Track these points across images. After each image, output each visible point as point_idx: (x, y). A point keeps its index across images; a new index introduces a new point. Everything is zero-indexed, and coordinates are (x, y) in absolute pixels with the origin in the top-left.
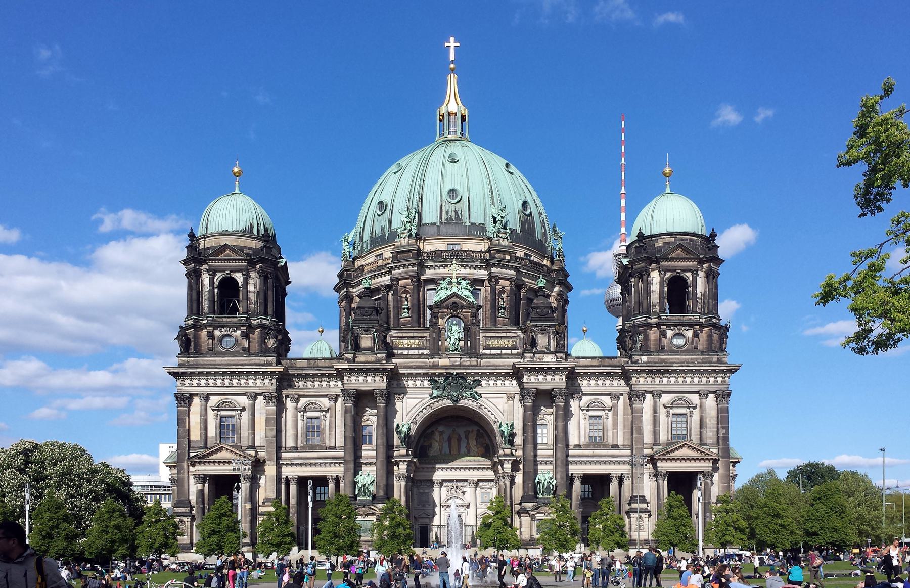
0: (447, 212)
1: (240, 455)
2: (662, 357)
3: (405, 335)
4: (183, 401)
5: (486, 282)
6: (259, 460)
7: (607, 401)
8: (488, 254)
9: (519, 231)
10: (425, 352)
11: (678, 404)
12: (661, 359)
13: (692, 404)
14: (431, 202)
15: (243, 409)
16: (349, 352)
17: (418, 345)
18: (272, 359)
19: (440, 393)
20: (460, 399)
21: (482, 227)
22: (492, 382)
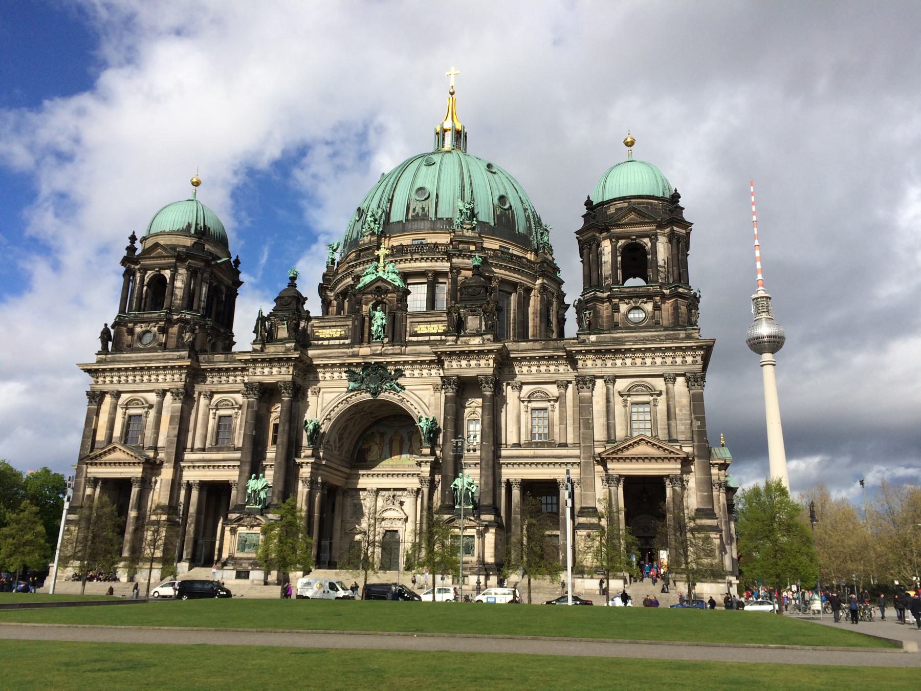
0: (414, 210)
1: (132, 456)
2: (614, 335)
3: (327, 324)
4: (94, 398)
5: (449, 274)
6: (155, 462)
7: (553, 390)
8: (451, 246)
9: (492, 224)
10: (347, 342)
11: (637, 391)
12: (613, 337)
13: (655, 390)
14: (400, 202)
15: (151, 407)
16: (258, 342)
17: (341, 335)
18: (185, 353)
19: (356, 385)
20: (380, 393)
21: (450, 221)
22: (416, 372)
